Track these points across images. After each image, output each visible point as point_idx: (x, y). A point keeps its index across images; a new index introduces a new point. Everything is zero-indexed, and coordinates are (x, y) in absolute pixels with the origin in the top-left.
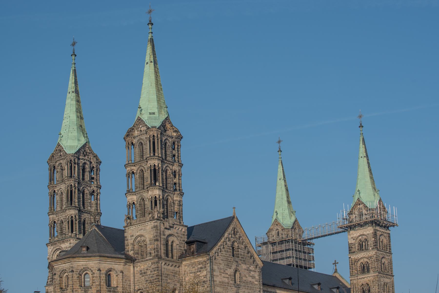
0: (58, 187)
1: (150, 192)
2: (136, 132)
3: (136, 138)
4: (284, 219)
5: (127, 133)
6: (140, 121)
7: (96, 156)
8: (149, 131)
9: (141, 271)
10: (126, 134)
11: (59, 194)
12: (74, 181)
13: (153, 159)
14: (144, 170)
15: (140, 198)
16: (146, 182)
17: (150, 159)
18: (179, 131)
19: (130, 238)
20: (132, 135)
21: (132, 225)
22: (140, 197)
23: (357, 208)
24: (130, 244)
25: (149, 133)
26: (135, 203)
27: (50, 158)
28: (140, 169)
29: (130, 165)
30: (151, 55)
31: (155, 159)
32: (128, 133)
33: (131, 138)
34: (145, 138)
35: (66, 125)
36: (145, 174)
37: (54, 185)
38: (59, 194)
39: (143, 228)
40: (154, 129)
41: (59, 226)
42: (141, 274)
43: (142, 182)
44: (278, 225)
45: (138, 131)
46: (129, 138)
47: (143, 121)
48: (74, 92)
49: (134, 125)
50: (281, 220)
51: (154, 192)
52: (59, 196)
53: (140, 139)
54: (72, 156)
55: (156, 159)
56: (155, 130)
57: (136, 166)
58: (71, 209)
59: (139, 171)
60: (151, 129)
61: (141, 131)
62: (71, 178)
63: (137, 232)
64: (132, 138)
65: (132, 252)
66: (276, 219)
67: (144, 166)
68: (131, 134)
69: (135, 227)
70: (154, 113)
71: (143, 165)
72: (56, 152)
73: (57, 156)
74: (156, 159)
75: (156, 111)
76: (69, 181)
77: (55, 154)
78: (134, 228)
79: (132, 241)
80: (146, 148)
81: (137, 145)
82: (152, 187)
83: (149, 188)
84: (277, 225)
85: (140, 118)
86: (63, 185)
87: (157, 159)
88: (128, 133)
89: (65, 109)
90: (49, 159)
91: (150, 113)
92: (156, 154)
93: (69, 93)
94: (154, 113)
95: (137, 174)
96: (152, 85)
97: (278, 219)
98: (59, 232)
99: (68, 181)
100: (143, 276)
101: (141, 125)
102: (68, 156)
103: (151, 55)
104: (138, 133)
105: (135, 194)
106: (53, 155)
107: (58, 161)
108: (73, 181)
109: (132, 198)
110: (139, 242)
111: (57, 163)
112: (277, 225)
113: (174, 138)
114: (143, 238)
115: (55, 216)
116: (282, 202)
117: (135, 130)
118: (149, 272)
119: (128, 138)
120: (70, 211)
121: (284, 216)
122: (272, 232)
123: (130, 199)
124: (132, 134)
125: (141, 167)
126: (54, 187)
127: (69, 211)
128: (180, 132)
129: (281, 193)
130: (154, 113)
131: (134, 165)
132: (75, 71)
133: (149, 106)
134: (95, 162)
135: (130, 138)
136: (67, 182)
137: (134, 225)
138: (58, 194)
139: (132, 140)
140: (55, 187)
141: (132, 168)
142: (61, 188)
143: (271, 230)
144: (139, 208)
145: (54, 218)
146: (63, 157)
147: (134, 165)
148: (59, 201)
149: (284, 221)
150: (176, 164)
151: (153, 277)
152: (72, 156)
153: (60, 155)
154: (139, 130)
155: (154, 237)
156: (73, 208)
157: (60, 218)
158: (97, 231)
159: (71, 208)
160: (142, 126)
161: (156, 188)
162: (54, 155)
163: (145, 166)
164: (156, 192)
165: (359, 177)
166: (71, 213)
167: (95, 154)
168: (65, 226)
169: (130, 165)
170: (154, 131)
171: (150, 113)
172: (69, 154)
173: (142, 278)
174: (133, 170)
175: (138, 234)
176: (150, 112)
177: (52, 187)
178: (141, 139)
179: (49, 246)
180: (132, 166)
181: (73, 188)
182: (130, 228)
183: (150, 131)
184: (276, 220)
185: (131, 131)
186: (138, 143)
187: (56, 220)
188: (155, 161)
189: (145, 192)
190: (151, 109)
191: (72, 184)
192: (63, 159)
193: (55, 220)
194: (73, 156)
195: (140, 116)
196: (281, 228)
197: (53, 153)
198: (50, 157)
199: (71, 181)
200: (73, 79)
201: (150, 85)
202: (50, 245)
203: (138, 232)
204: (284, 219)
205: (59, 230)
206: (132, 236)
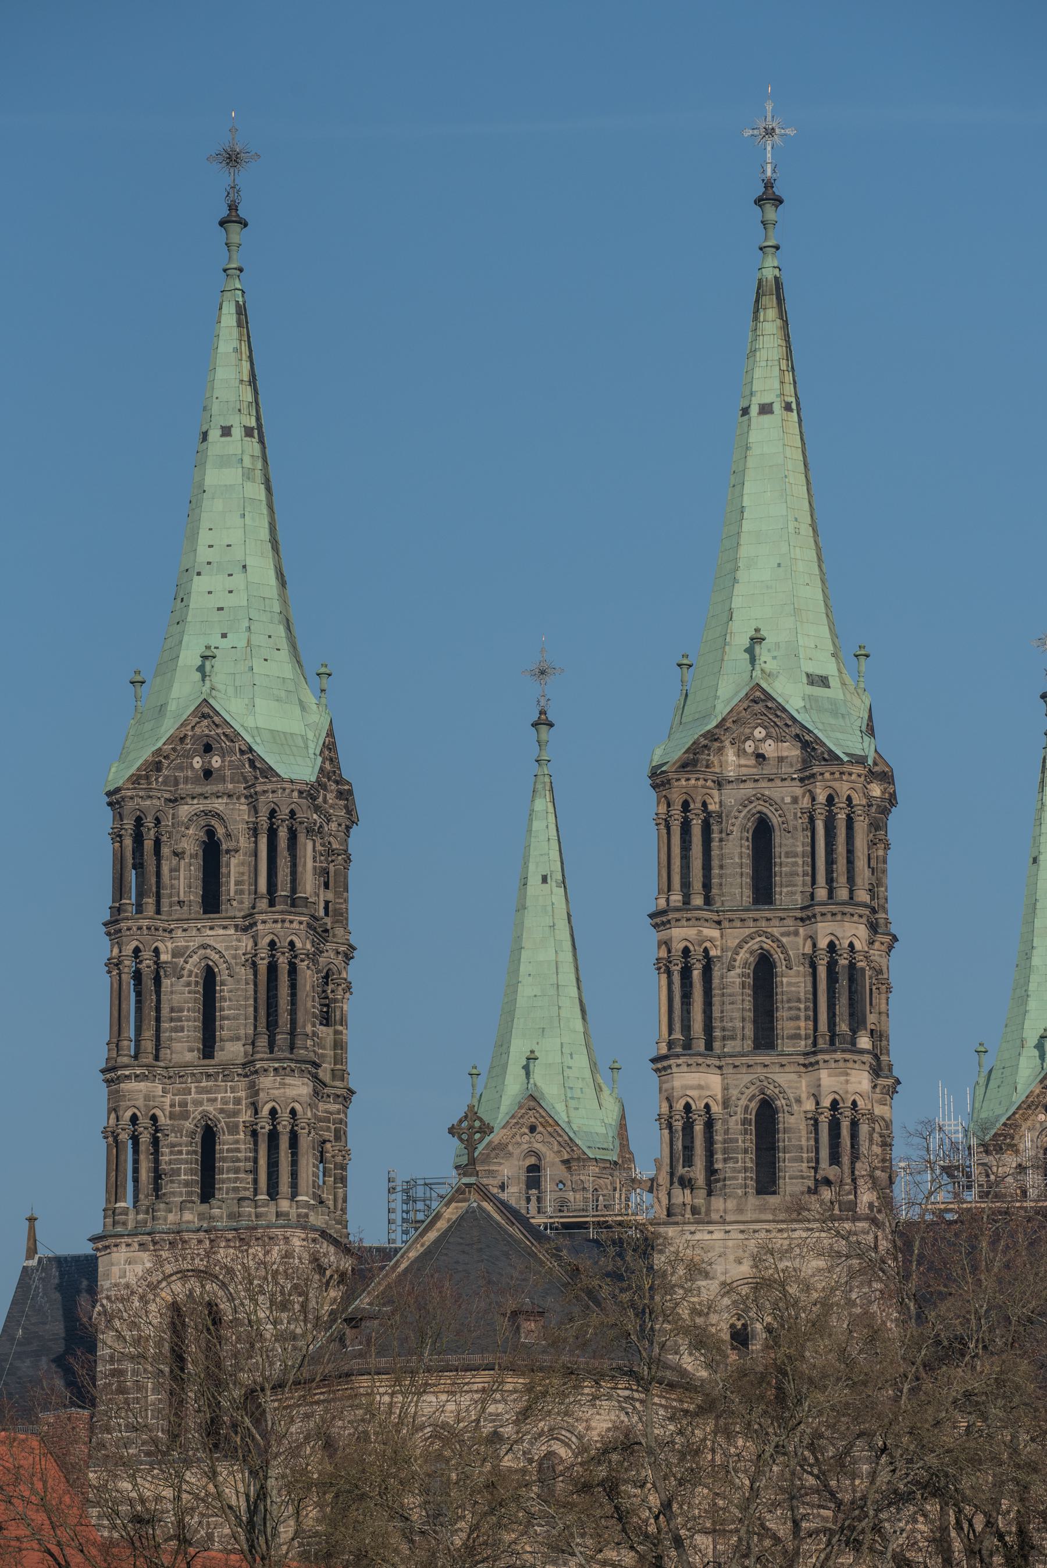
0: (179, 933)
1: (830, 1076)
2: (730, 755)
3: (734, 786)
4: (572, 1104)
5: (685, 753)
6: (757, 708)
7: (350, 792)
8: (827, 775)
10: (680, 758)
11: (190, 976)
12: (309, 926)
13: (848, 916)
14: (778, 956)
15: (747, 1091)
16: (791, 1019)
17: (834, 914)
18: (892, 776)
20: (707, 767)
21: (709, 1223)
22: (753, 1087)
23: (1029, 1123)
25: (829, 784)
26: (715, 1109)
27: (138, 769)
28: (753, 944)
29: (697, 919)
30: (786, 373)
31: (856, 918)
32: (691, 756)
33: (706, 780)
34: (788, 800)
35: (221, 609)
36: (785, 980)
37: (159, 924)
38: (191, 972)
40: (858, 769)
41: (184, 1149)
43: (809, 1029)
44: (540, 1129)
45: (741, 753)
46: (701, 782)
47: (784, 710)
48: (252, 436)
49: (724, 720)
50: (560, 1107)
51: (852, 1079)
52: (189, 984)
53: (758, 799)
54: (301, 792)
55: (861, 920)
56: (859, 776)
57: (726, 924)
58: (293, 1071)
59: (743, 955)
60: (847, 768)
61: (760, 757)
62: (293, 909)
64: (709, 783)
66: (535, 1094)
67: (783, 934)
68: (704, 763)
69: (727, 1232)
70: (823, 681)
71: (776, 931)
72: (179, 748)
73: (180, 768)
74: (861, 916)
76: (283, 921)
77: (172, 757)
78: (715, 1236)
80: (793, 849)
81: (738, 822)
82: (848, 1056)
83: (827, 1057)
84: (533, 1129)
85: (764, 691)
86: (221, 932)
87: (864, 920)
88: (691, 756)
89: (204, 516)
90: (133, 775)
91: (808, 675)
92: (843, 894)
93: (226, 431)
94: (826, 678)
95: (734, 967)
96: (802, 532)
97: (544, 1099)
98: (183, 1177)
99: (275, 921)
101: (759, 729)
102: (284, 789)
103: (786, 373)
104: (743, 762)
105: (720, 1068)
106: (160, 762)
107: (195, 801)
108: (302, 926)
109: (702, 1083)
111: (185, 811)
112: (533, 1129)
113: (875, 807)
115: (161, 1086)
116: (559, 1008)
117: (727, 743)
119: (688, 779)
120: (289, 1080)
121: (571, 1088)
122: (501, 1164)
123: (692, 1088)
124: (708, 760)
125: (759, 939)
126: (157, 933)
127: (285, 1084)
128: (894, 784)
129: (553, 958)
130: (826, 678)
131: (716, 918)
132: (241, 311)
133: (801, 642)
134: (340, 825)
135: (701, 782)
136: (268, 926)
137: (724, 1222)
138: (185, 972)
139: (709, 791)
140: (165, 930)
142: (204, 947)
143: (494, 1149)
144: (740, 1138)
145: (154, 1097)
146: (230, 786)
147: (719, 923)
148: (185, 1013)
149: (572, 1113)
150: (883, 940)
152: (301, 792)
153: (208, 773)
154: (750, 750)
156: (303, 1066)
157: (198, 1103)
158: (498, 1223)
159: (293, 1065)
160: (768, 736)
161: (859, 1062)
162: (165, 762)
163: (784, 940)
164: (860, 1083)
165: (1036, 961)
166: (291, 1092)
167: (348, 783)
168: (228, 1150)
169: (697, 919)
170: (854, 777)
171: (808, 675)
172: (292, 782)
174: (708, 944)
176: (810, 671)
177: (149, 928)
178: (768, 800)
179: (123, 1248)
180: (706, 924)
181: (302, 961)
182: (692, 1233)
183: (837, 775)
184: (532, 1104)
185: (705, 746)
186: (743, 814)
187: (163, 1110)
188: (857, 928)
189: (787, 1069)
190: (810, 659)
191: (294, 938)
192: (230, 796)
193: (158, 1113)
194: (304, 795)
195: (764, 685)
196: (556, 1147)
197: (160, 749)
198: (142, 765)
199: (295, 925)
200: (244, 357)
201: (791, 529)
202: (128, 1245)
203: (740, 1263)
204: (572, 1104)
205: (183, 1166)
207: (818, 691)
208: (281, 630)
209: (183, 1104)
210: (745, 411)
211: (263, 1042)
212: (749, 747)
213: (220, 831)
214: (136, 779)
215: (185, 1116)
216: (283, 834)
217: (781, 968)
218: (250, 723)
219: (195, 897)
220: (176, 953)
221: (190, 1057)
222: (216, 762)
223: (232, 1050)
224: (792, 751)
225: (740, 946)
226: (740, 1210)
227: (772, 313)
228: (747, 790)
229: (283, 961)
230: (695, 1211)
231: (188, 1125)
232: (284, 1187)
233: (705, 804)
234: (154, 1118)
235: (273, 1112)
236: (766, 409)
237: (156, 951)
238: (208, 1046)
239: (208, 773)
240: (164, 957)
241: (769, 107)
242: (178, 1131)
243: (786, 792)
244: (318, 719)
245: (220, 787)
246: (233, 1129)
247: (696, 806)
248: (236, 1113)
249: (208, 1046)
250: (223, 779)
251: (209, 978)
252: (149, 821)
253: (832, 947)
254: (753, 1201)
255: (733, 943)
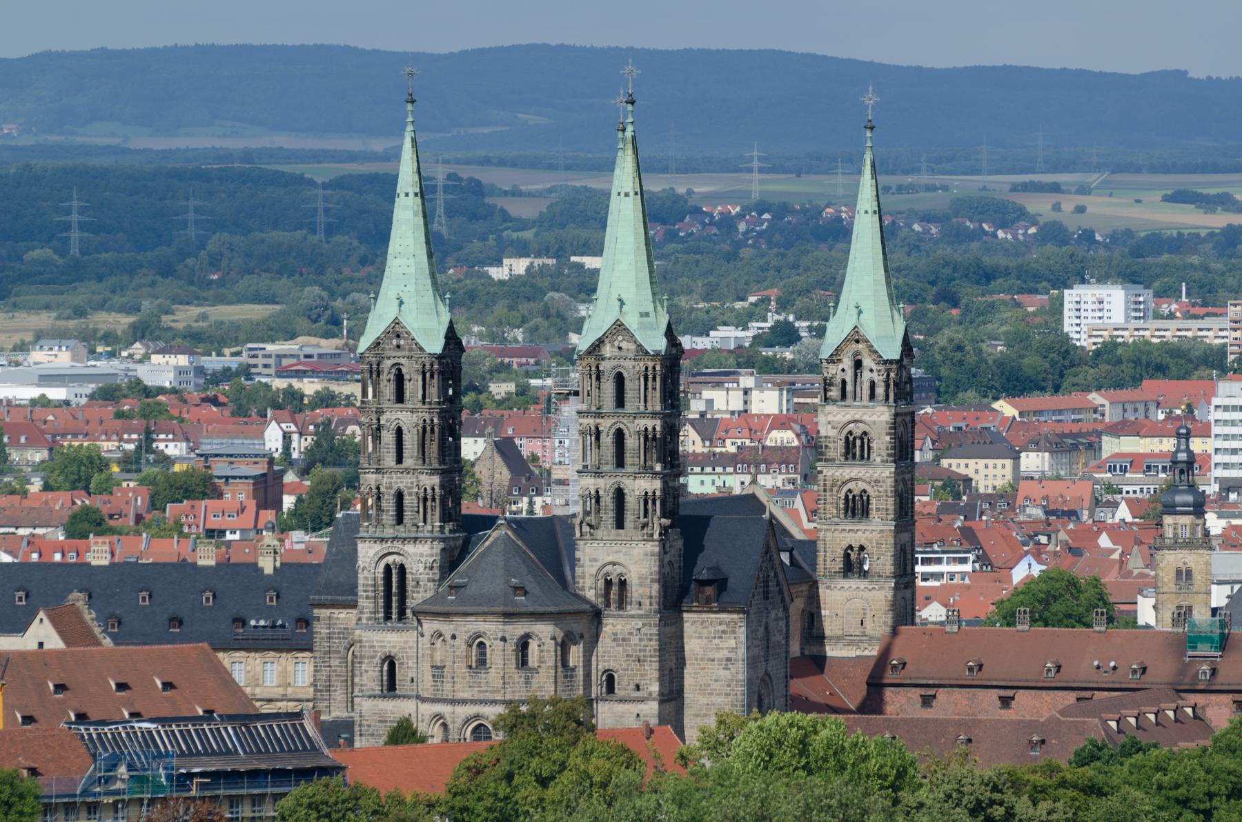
9: (615, 634)
14: (626, 431)
19: (587, 563)
24: (587, 575)
26: (601, 493)
28: (616, 427)
39: (624, 550)
42: (615, 640)
45: (613, 346)
59: (613, 431)
61: (620, 348)
63: (608, 555)
65: (593, 592)
70: (647, 314)
71: (625, 421)
75: (650, 308)
79: (594, 571)
100: (618, 645)
110: (607, 574)
114: (619, 569)
118: (635, 640)
141: (598, 421)
151: (645, 650)
155: (651, 574)
173: (617, 649)
175: (610, 559)
206: (595, 560)
207: (645, 320)
208: (429, 282)
209: (391, 483)
210: (619, 194)
211: (420, 462)
212: (616, 343)
213: (404, 370)
214: (369, 349)
215: (391, 488)
216: (428, 375)
217: (627, 436)
218: (416, 326)
219: (393, 397)
220: (387, 421)
221: (393, 464)
222: (402, 342)
223: (408, 462)
224: (632, 347)
225: (611, 427)
226: (609, 535)
227: (630, 152)
228: (615, 362)
229: (428, 428)
230: (591, 535)
231: (393, 492)
232: (429, 520)
233: (597, 367)
234: (378, 488)
235: (425, 489)
236: (627, 195)
237: (379, 420)
238: (399, 460)
239: (398, 346)
240: (382, 422)
241: (630, 61)
242: (389, 494)
243: (629, 364)
244: (446, 318)
245: (403, 353)
246: (410, 494)
247: (593, 369)
248: (412, 488)
249: (399, 460)
250: (404, 350)
251: (399, 431)
252: (374, 366)
253: (646, 429)
254: (614, 532)
255: (609, 425)
